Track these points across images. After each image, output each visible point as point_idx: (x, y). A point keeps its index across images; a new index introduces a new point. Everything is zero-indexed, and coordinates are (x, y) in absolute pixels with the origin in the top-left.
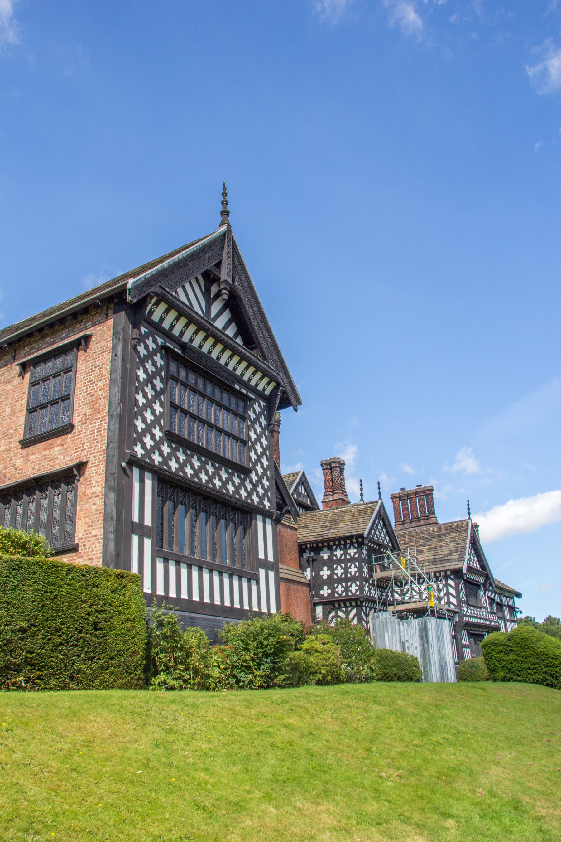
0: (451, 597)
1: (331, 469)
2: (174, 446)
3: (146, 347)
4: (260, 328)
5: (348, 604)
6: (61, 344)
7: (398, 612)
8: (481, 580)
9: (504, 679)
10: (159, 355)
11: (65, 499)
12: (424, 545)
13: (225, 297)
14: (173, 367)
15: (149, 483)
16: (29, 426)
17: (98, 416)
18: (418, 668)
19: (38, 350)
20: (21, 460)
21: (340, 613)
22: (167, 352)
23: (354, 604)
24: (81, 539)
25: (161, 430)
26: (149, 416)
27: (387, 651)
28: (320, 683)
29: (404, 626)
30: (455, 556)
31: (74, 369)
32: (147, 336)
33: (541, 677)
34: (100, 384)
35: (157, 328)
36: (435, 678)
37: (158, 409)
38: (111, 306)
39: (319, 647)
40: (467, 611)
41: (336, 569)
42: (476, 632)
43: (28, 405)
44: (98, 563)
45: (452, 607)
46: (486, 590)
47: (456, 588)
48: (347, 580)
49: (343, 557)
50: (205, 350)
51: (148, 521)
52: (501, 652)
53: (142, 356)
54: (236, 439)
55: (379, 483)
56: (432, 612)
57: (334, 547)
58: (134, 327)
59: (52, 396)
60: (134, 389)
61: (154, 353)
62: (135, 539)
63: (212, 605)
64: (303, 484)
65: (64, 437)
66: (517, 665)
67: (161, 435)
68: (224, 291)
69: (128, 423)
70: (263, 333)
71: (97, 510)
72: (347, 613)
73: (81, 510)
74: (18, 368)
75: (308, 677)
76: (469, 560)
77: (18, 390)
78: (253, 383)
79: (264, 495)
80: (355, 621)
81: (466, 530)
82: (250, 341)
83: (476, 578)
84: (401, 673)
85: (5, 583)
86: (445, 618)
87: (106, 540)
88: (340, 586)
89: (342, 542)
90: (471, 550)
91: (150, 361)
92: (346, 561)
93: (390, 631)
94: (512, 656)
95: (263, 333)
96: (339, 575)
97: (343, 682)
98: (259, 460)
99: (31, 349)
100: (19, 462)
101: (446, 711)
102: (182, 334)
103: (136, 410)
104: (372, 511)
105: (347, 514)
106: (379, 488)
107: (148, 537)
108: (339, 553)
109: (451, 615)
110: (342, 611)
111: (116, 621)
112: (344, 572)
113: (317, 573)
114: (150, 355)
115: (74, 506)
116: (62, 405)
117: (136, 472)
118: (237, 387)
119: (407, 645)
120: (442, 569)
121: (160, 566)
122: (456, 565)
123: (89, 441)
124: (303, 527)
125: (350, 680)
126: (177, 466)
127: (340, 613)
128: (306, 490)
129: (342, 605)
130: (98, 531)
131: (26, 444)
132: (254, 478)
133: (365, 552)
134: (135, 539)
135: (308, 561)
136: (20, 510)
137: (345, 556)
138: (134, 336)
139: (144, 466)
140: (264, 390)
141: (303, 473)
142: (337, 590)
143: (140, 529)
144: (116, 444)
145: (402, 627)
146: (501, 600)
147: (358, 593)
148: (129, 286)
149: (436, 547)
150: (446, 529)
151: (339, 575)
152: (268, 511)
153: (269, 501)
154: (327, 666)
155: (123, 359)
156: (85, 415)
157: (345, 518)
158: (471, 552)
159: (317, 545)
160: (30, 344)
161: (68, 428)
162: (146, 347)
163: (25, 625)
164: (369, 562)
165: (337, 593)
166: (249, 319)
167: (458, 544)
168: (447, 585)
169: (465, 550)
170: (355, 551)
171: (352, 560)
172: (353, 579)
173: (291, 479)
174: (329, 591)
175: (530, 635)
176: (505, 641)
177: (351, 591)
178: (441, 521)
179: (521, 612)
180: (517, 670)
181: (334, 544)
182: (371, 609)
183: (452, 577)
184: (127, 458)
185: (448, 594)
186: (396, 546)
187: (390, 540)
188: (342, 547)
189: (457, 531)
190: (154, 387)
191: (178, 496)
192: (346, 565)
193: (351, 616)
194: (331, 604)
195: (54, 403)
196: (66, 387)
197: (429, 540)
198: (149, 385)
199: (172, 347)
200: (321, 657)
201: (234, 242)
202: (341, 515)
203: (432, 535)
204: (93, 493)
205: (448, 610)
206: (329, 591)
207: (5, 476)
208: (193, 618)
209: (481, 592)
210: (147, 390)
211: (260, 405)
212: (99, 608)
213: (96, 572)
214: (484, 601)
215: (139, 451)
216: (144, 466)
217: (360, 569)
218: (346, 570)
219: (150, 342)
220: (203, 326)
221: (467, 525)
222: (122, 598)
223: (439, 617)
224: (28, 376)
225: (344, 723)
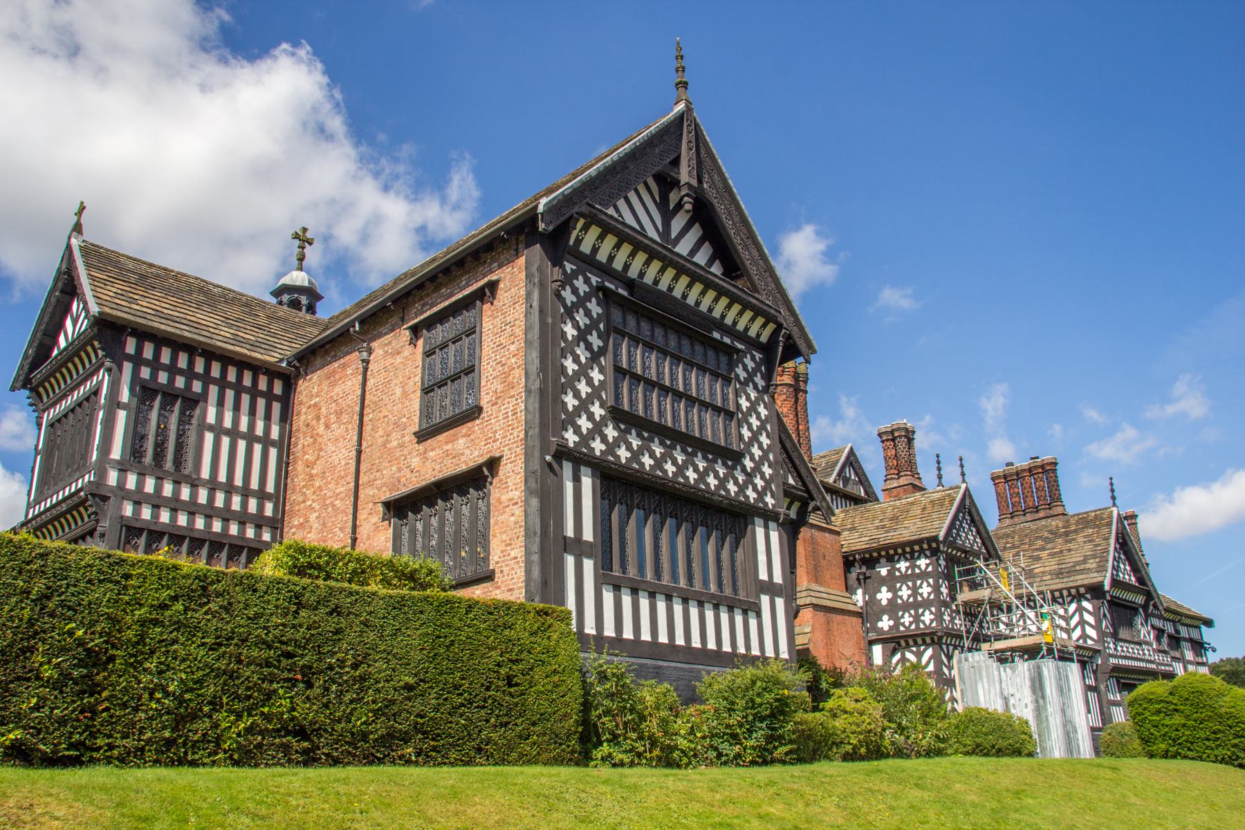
1: (893, 440)
2: (623, 427)
3: (575, 291)
4: (746, 247)
5: (919, 641)
6: (460, 296)
7: (996, 651)
8: (1140, 600)
9: (1166, 755)
10: (594, 300)
11: (474, 510)
12: (1043, 549)
13: (688, 207)
14: (617, 315)
15: (587, 482)
16: (426, 411)
17: (512, 392)
18: (1031, 737)
19: (432, 306)
21: (909, 655)
22: (606, 297)
23: (928, 640)
25: (601, 406)
26: (584, 388)
27: (979, 710)
28: (847, 757)
29: (1006, 672)
30: (1092, 564)
31: (478, 329)
32: (574, 275)
34: (512, 348)
35: (589, 262)
36: (1057, 750)
37: (596, 376)
38: (522, 238)
39: (849, 704)
41: (900, 589)
42: (1126, 679)
43: (423, 383)
44: (518, 596)
45: (1090, 642)
46: (1147, 616)
48: (916, 605)
51: (588, 535)
52: (1158, 712)
53: (569, 304)
54: (718, 410)
56: (1050, 651)
58: (554, 266)
59: (452, 368)
60: (559, 351)
61: (587, 297)
62: (570, 560)
63: (688, 648)
64: (851, 464)
65: (469, 424)
67: (603, 412)
68: (686, 199)
69: (553, 400)
70: (750, 254)
71: (516, 523)
72: (919, 655)
73: (496, 524)
74: (407, 333)
75: (830, 749)
76: (1116, 568)
79: (764, 488)
80: (931, 668)
81: (1110, 524)
82: (733, 268)
83: (1129, 596)
84: (1002, 743)
85: (382, 626)
86: (1071, 660)
87: (528, 563)
88: (907, 615)
89: (908, 549)
91: (581, 310)
92: (914, 577)
93: (985, 680)
94: (1178, 719)
95: (750, 254)
96: (905, 598)
97: (887, 756)
98: (755, 437)
99: (423, 306)
100: (415, 461)
101: (1030, 801)
102: (627, 267)
103: (563, 380)
104: (952, 501)
105: (914, 507)
107: (589, 557)
108: (903, 565)
109: (1085, 657)
110: (912, 652)
111: (538, 674)
112: (911, 593)
113: (873, 597)
114: (581, 302)
115: (487, 517)
116: (465, 380)
117: (567, 468)
118: (716, 335)
119: (1012, 701)
120: (1071, 584)
121: (608, 597)
122: (1093, 578)
123: (501, 429)
124: (850, 530)
125: (900, 753)
126: (629, 455)
127: (909, 655)
128: (856, 474)
129: (911, 642)
130: (518, 552)
131: (423, 436)
132: (749, 464)
133: (942, 563)
134: (570, 560)
135: (858, 579)
136: (419, 526)
137: (913, 570)
138: (555, 278)
139: (579, 458)
140: (758, 335)
141: (851, 451)
143: (577, 547)
144: (537, 430)
145: (1003, 674)
146: (1177, 631)
147: (934, 624)
148: (541, 209)
149: (1061, 552)
150: (1077, 523)
151: (905, 598)
152: (771, 511)
153: (772, 496)
154: (860, 733)
155: (541, 311)
156: (496, 392)
157: (912, 513)
160: (421, 298)
161: (475, 412)
162: (575, 291)
163: (411, 680)
164: (949, 577)
165: (903, 624)
166: (728, 235)
167: (1096, 546)
168: (1080, 609)
170: (928, 561)
171: (924, 575)
172: (926, 604)
173: (833, 458)
174: (891, 623)
175: (1207, 686)
177: (923, 622)
178: (1070, 511)
179: (1214, 650)
180: (1187, 741)
181: (896, 553)
182: (955, 647)
184: (553, 449)
185: (1082, 622)
186: (993, 552)
187: (983, 543)
189: (1097, 526)
190: (589, 347)
191: (632, 497)
192: (914, 584)
193: (924, 659)
194: (895, 642)
195: (455, 378)
196: (470, 355)
197: (1051, 541)
198: (582, 344)
199: (613, 287)
200: (851, 720)
201: (696, 125)
202: (906, 510)
203: (1055, 534)
204: (510, 500)
205: (1078, 647)
206: (891, 623)
208: (660, 667)
209: (1139, 620)
210: (578, 352)
211: (753, 359)
212: (514, 657)
213: (509, 609)
214: (1145, 632)
215: (571, 438)
216: (579, 458)
217: (936, 589)
218: (915, 591)
219: (579, 283)
220: (660, 254)
221: (1110, 516)
222: (545, 642)
223: (1062, 659)
224: (420, 342)
225: (855, 814)
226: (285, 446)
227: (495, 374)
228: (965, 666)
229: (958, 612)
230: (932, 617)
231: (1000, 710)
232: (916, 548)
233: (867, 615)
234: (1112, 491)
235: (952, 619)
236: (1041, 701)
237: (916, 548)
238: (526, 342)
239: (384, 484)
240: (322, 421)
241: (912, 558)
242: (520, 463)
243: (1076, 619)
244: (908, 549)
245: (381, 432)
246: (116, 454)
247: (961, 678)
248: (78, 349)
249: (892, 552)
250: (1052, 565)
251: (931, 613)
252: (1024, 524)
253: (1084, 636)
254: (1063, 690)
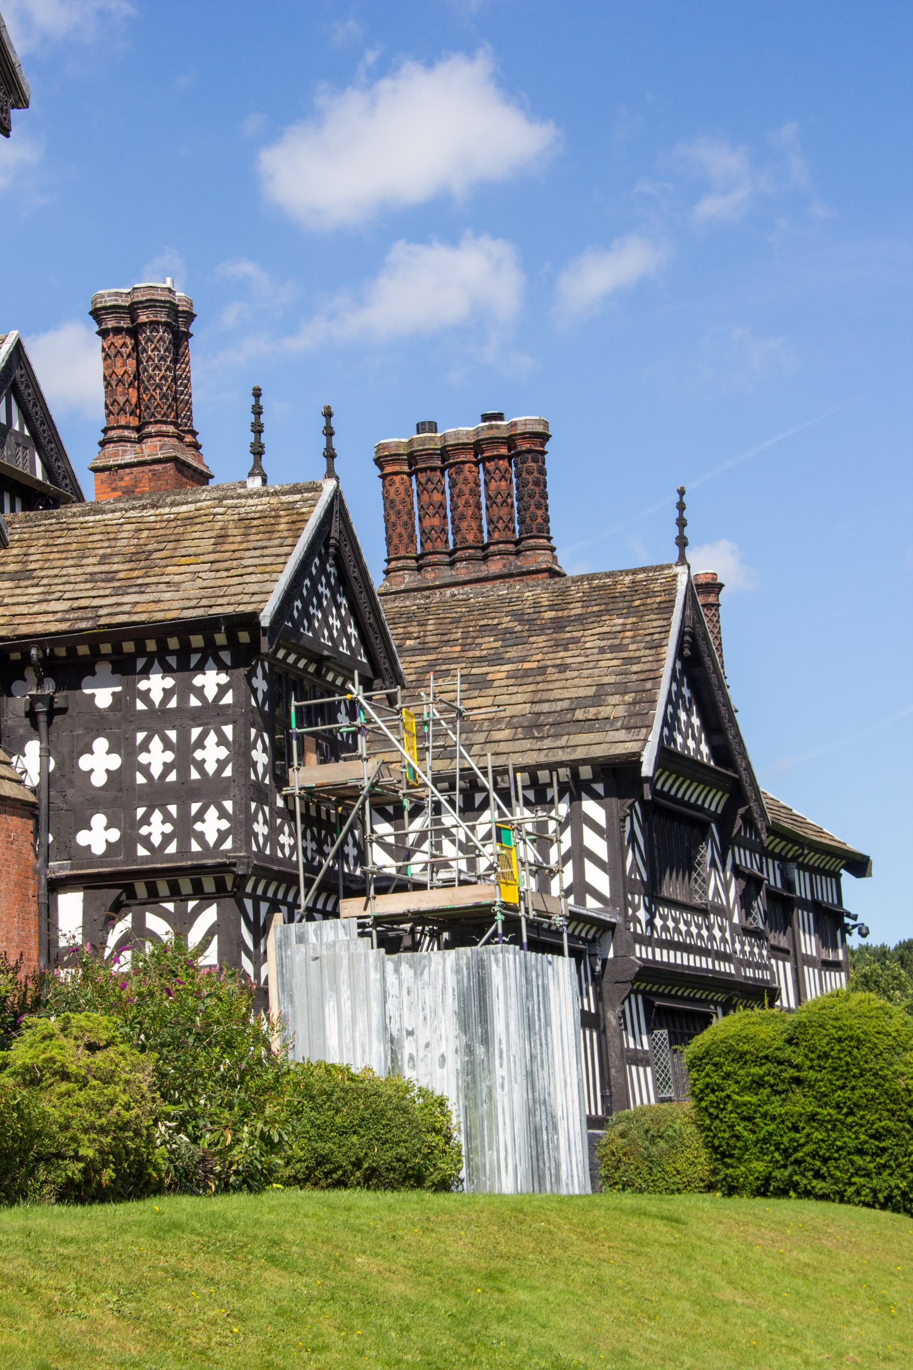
0: (589, 865)
5: (186, 886)
7: (379, 920)
8: (714, 802)
9: (764, 1189)
12: (496, 659)
18: (448, 1138)
21: (154, 922)
23: (209, 885)
27: (329, 1069)
29: (401, 970)
30: (615, 707)
33: (903, 1185)
36: (508, 1177)
40: (650, 923)
41: (145, 747)
42: (676, 1003)
45: (592, 903)
48: (186, 792)
49: (173, 704)
52: (758, 1083)
55: (328, 414)
56: (512, 924)
57: (141, 663)
66: (818, 1135)
72: (182, 923)
76: (670, 722)
80: (211, 957)
81: (666, 608)
83: (692, 793)
84: (380, 1156)
86: (559, 951)
88: (157, 816)
89: (173, 643)
90: (680, 685)
92: (183, 718)
93: (345, 993)
96: (156, 771)
105: (195, 531)
106: (329, 433)
108: (156, 685)
109: (584, 940)
110: (164, 915)
112: (174, 760)
113: (68, 764)
119: (408, 1047)
122: (614, 744)
127: (154, 922)
129: (163, 888)
133: (261, 684)
135: (31, 715)
142: (144, 831)
145: (391, 977)
146: (788, 884)
149: (542, 670)
150: (586, 601)
158: (679, 694)
159: (72, 651)
164: (273, 722)
165: (146, 841)
167: (628, 661)
168: (577, 820)
169: (657, 686)
170: (224, 678)
171: (211, 715)
172: (211, 790)
174: (114, 835)
175: (871, 1026)
176: (779, 1043)
177: (200, 837)
180: (814, 1155)
181: (141, 651)
182: (274, 908)
183: (599, 788)
186: (384, 664)
187: (363, 638)
188: (172, 661)
189: (631, 611)
192: (184, 736)
193: (195, 936)
194: (120, 887)
203: (531, 623)
205: (573, 917)
206: (114, 835)
209: (707, 853)
214: (719, 886)
217: (240, 752)
218: (184, 753)
221: (670, 590)
223: (536, 946)
228: (298, 954)
229: (290, 815)
230: (225, 825)
231: (379, 1070)
232: (197, 641)
233: (49, 812)
235: (275, 831)
236: (480, 1050)
237: (197, 641)
241: (183, 665)
244: (173, 643)
247: (285, 987)
249: (129, 647)
250: (518, 703)
251: (223, 814)
252: (465, 593)
254: (533, 1024)
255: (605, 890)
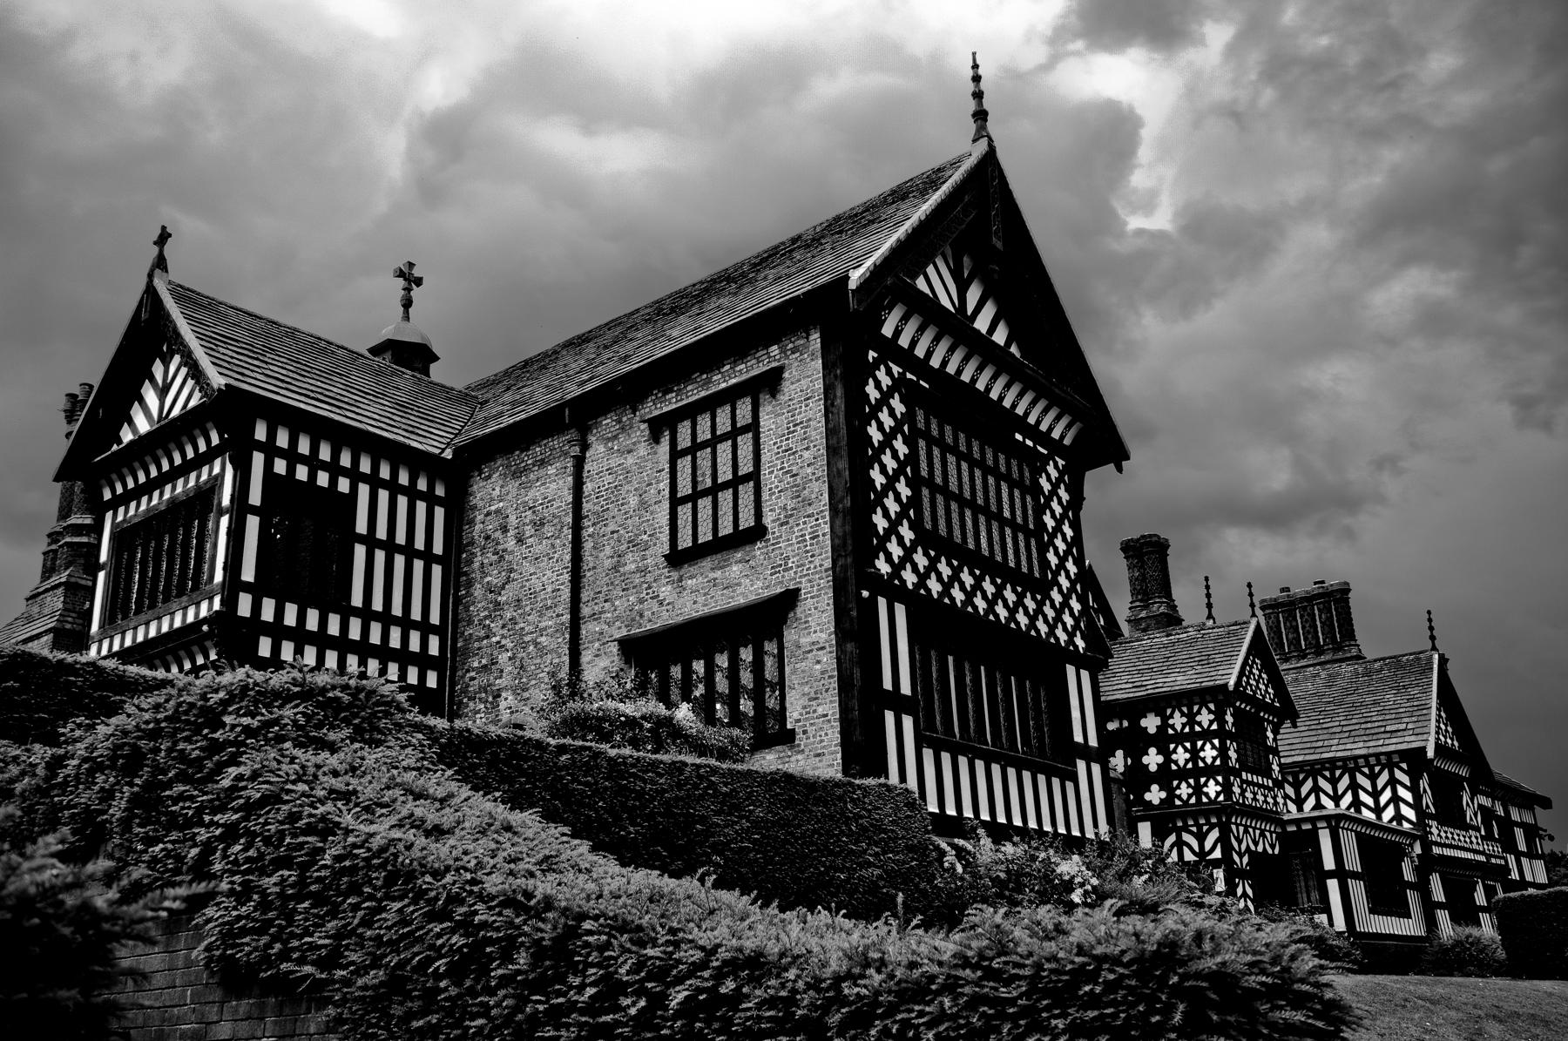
0: (1402, 806)
10: (896, 395)
20: (669, 587)
21: (1186, 837)
24: (798, 721)
34: (806, 454)
41: (1175, 751)
45: (1406, 825)
47: (1414, 789)
48: (1200, 772)
49: (1187, 730)
50: (966, 377)
55: (1249, 585)
71: (823, 673)
72: (1201, 837)
73: (794, 671)
77: (649, 464)
78: (1044, 427)
80: (1217, 854)
88: (1184, 785)
96: (1181, 763)
118: (1019, 437)
123: (797, 554)
127: (1186, 837)
130: (830, 707)
131: (677, 559)
132: (1056, 597)
147: (1221, 798)
151: (1181, 763)
161: (758, 532)
165: (1179, 797)
172: (1210, 771)
174: (1163, 795)
177: (1207, 795)
178: (1369, 654)
179: (1551, 838)
185: (1396, 799)
193: (1208, 845)
206: (1163, 795)
207: (641, 616)
215: (883, 567)
216: (896, 592)
217: (1223, 752)
218: (1195, 754)
226: (455, 563)
227: (781, 486)
230: (1219, 788)
234: (1431, 628)
238: (828, 447)
239: (618, 618)
240: (511, 533)
242: (827, 598)
243: (1384, 798)
245: (608, 551)
246: (248, 575)
248: (170, 433)
251: (1217, 783)
253: (1398, 817)
255: (1413, 818)
